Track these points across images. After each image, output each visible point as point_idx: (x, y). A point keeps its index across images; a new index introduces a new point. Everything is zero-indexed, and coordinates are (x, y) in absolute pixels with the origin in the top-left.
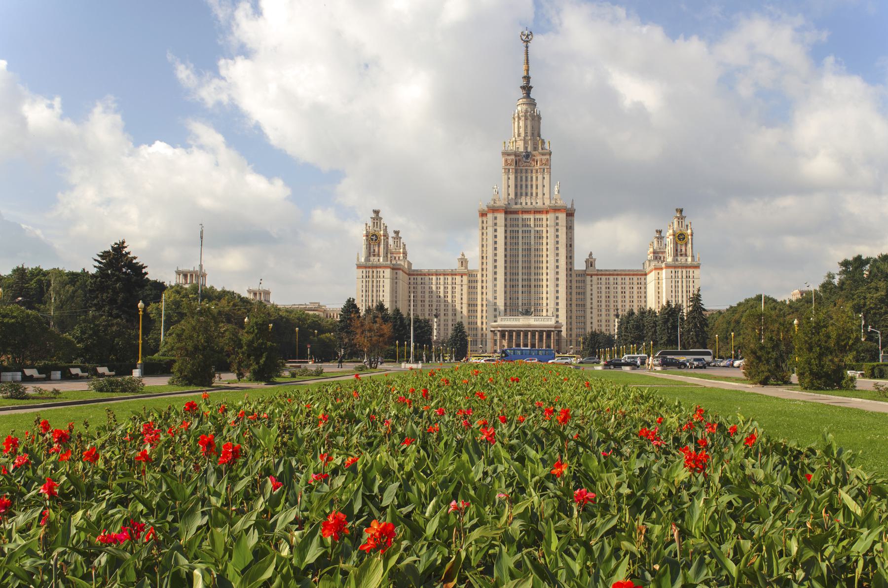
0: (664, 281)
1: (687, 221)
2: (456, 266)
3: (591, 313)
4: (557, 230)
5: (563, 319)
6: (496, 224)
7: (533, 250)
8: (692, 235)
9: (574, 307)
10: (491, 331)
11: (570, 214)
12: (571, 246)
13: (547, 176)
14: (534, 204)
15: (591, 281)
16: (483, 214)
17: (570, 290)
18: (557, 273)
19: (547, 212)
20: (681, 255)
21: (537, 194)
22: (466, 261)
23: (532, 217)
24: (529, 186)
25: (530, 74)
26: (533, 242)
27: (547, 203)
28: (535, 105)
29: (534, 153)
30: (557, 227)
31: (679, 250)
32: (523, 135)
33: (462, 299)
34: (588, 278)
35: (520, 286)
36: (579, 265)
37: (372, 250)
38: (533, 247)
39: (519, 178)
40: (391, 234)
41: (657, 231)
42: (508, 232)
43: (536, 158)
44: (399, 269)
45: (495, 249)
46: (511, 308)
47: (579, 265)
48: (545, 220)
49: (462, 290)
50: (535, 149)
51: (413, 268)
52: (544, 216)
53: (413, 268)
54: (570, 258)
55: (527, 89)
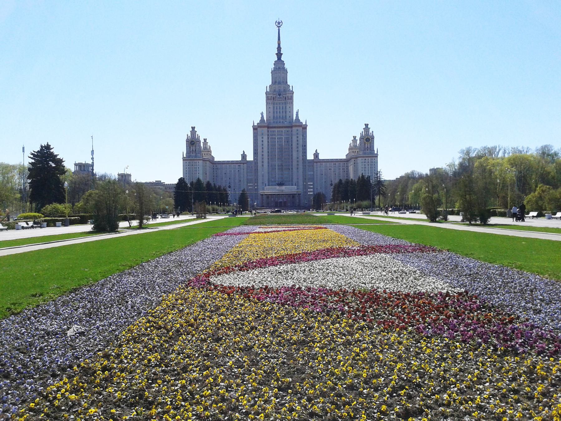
1: (371, 131)
2: (239, 158)
4: (297, 137)
5: (301, 187)
11: (305, 128)
12: (305, 146)
14: (284, 121)
15: (317, 165)
16: (255, 128)
19: (291, 127)
20: (368, 150)
21: (286, 116)
22: (246, 156)
23: (283, 130)
24: (281, 112)
25: (281, 46)
26: (283, 144)
28: (284, 64)
34: (315, 164)
35: (277, 169)
36: (310, 156)
37: (191, 149)
38: (284, 147)
40: (202, 141)
42: (270, 138)
43: (285, 96)
45: (263, 148)
47: (310, 156)
48: (290, 131)
51: (215, 160)
52: (290, 129)
53: (215, 160)
55: (279, 55)
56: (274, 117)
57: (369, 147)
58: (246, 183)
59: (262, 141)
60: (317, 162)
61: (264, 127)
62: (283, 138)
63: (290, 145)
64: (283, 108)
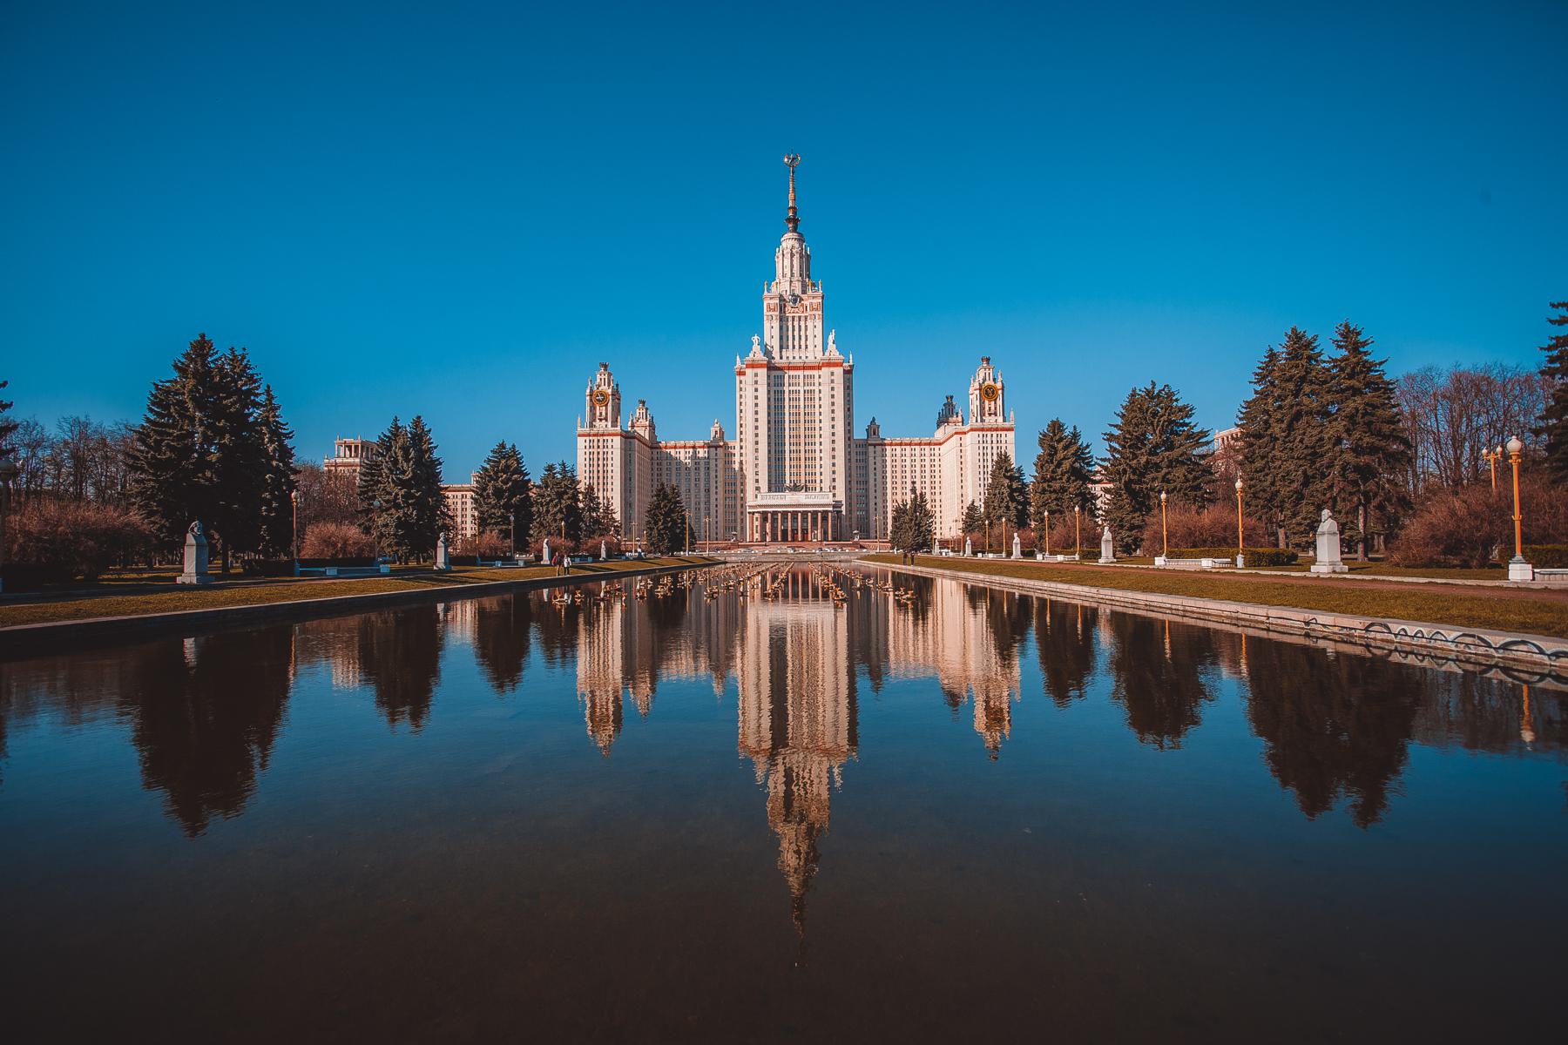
0: (969, 448)
3: (875, 491)
4: (833, 389)
5: (841, 497)
6: (756, 382)
7: (802, 414)
8: (1003, 389)
9: (854, 484)
10: (749, 513)
13: (819, 324)
14: (804, 358)
15: (875, 452)
17: (848, 457)
18: (833, 442)
19: (819, 368)
20: (990, 415)
23: (801, 373)
27: (819, 355)
29: (803, 296)
30: (832, 385)
31: (987, 409)
32: (789, 275)
33: (716, 476)
34: (871, 449)
37: (598, 414)
39: (784, 326)
41: (947, 398)
42: (772, 393)
44: (634, 438)
45: (756, 413)
46: (776, 484)
47: (860, 434)
48: (817, 377)
49: (716, 465)
50: (804, 292)
52: (815, 373)
54: (849, 424)
55: (795, 221)
56: (781, 348)
57: (993, 408)
58: (720, 489)
59: (756, 398)
60: (875, 445)
61: (761, 366)
62: (802, 392)
63: (817, 406)
64: (800, 330)
